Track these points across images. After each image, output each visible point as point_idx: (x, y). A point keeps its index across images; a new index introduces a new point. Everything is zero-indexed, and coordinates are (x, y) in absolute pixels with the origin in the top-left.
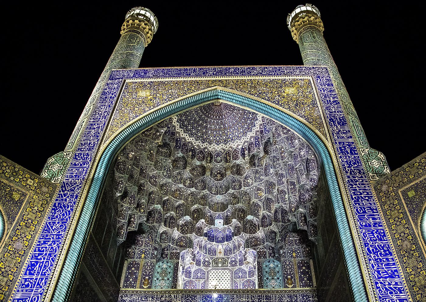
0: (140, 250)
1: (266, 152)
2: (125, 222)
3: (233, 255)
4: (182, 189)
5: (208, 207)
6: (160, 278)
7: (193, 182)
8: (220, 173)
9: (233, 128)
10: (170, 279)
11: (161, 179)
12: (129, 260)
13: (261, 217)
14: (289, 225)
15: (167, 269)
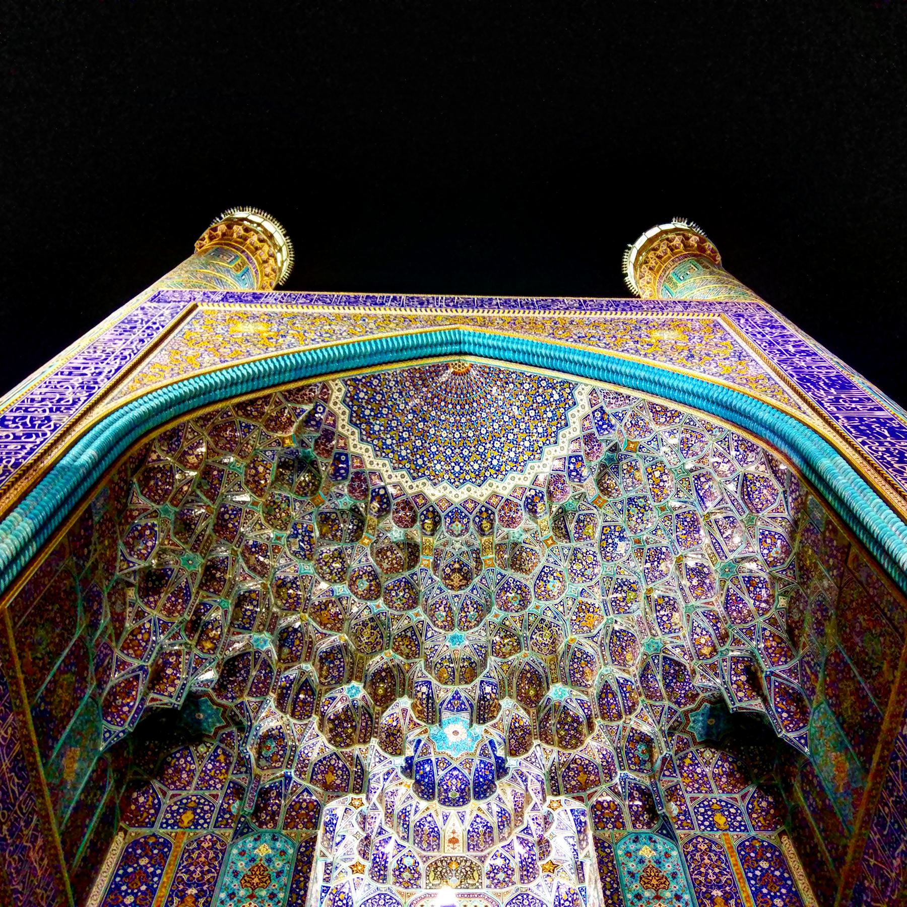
0: (181, 801)
1: (605, 490)
2: (141, 668)
3: (498, 846)
4: (344, 602)
5: (422, 663)
6: (242, 893)
7: (378, 585)
8: (460, 570)
9: (503, 439)
10: (281, 895)
11: (282, 561)
12: (133, 831)
13: (594, 691)
14: (692, 710)
15: (269, 860)
